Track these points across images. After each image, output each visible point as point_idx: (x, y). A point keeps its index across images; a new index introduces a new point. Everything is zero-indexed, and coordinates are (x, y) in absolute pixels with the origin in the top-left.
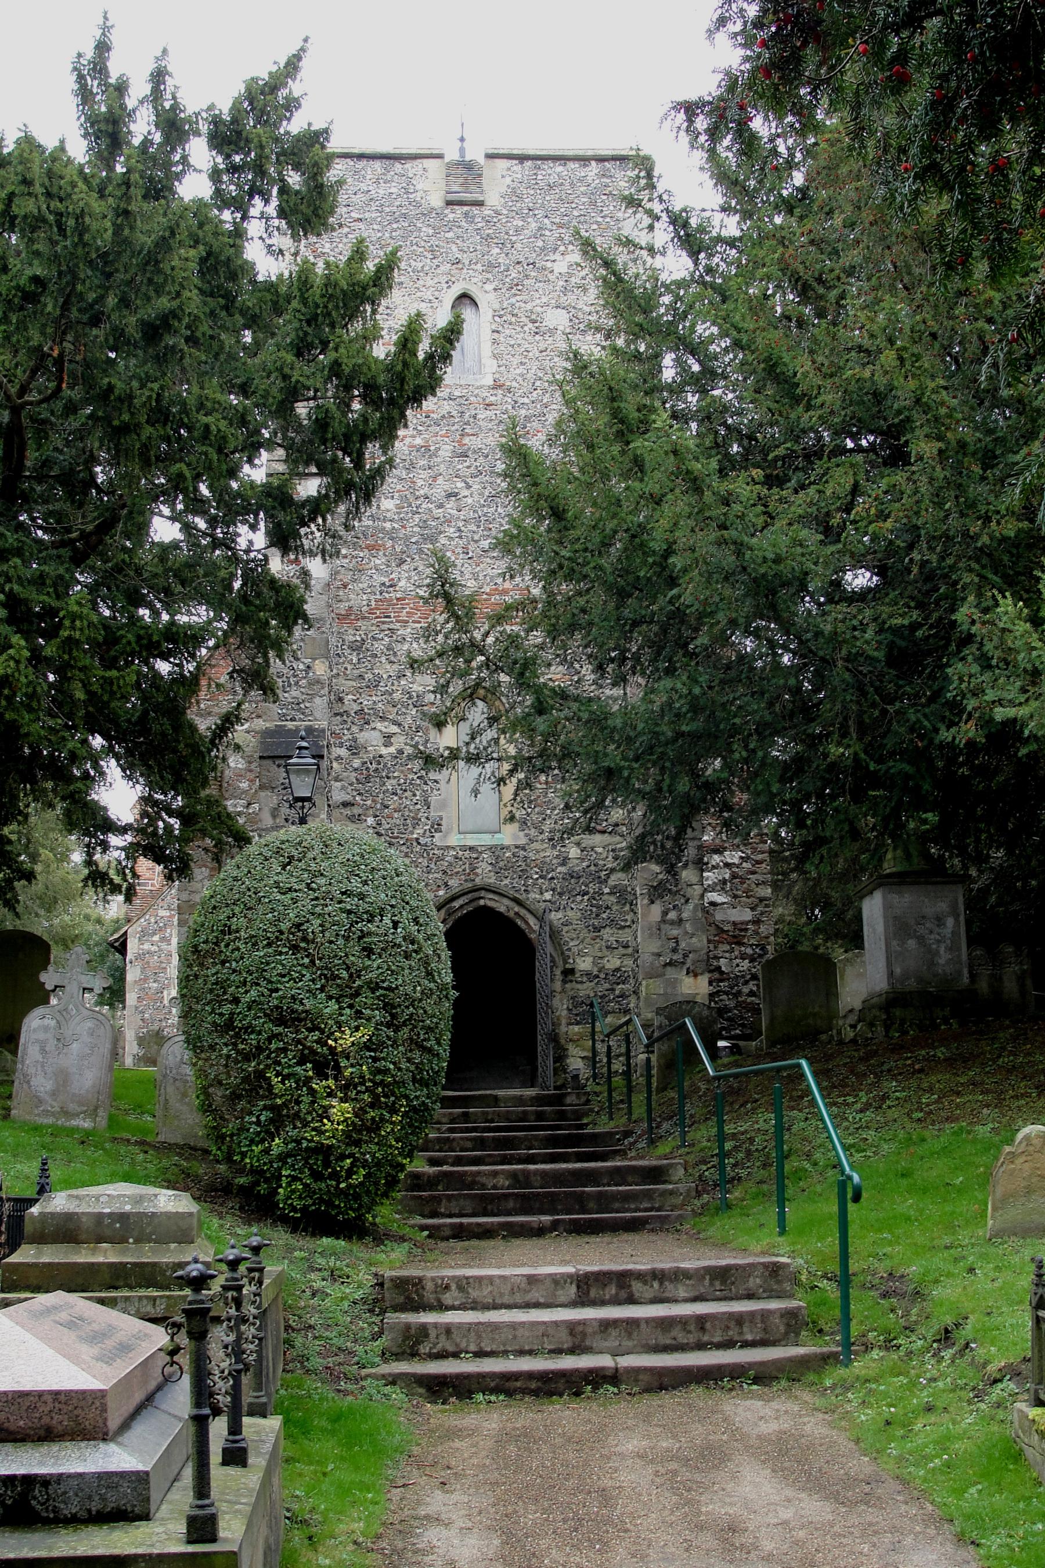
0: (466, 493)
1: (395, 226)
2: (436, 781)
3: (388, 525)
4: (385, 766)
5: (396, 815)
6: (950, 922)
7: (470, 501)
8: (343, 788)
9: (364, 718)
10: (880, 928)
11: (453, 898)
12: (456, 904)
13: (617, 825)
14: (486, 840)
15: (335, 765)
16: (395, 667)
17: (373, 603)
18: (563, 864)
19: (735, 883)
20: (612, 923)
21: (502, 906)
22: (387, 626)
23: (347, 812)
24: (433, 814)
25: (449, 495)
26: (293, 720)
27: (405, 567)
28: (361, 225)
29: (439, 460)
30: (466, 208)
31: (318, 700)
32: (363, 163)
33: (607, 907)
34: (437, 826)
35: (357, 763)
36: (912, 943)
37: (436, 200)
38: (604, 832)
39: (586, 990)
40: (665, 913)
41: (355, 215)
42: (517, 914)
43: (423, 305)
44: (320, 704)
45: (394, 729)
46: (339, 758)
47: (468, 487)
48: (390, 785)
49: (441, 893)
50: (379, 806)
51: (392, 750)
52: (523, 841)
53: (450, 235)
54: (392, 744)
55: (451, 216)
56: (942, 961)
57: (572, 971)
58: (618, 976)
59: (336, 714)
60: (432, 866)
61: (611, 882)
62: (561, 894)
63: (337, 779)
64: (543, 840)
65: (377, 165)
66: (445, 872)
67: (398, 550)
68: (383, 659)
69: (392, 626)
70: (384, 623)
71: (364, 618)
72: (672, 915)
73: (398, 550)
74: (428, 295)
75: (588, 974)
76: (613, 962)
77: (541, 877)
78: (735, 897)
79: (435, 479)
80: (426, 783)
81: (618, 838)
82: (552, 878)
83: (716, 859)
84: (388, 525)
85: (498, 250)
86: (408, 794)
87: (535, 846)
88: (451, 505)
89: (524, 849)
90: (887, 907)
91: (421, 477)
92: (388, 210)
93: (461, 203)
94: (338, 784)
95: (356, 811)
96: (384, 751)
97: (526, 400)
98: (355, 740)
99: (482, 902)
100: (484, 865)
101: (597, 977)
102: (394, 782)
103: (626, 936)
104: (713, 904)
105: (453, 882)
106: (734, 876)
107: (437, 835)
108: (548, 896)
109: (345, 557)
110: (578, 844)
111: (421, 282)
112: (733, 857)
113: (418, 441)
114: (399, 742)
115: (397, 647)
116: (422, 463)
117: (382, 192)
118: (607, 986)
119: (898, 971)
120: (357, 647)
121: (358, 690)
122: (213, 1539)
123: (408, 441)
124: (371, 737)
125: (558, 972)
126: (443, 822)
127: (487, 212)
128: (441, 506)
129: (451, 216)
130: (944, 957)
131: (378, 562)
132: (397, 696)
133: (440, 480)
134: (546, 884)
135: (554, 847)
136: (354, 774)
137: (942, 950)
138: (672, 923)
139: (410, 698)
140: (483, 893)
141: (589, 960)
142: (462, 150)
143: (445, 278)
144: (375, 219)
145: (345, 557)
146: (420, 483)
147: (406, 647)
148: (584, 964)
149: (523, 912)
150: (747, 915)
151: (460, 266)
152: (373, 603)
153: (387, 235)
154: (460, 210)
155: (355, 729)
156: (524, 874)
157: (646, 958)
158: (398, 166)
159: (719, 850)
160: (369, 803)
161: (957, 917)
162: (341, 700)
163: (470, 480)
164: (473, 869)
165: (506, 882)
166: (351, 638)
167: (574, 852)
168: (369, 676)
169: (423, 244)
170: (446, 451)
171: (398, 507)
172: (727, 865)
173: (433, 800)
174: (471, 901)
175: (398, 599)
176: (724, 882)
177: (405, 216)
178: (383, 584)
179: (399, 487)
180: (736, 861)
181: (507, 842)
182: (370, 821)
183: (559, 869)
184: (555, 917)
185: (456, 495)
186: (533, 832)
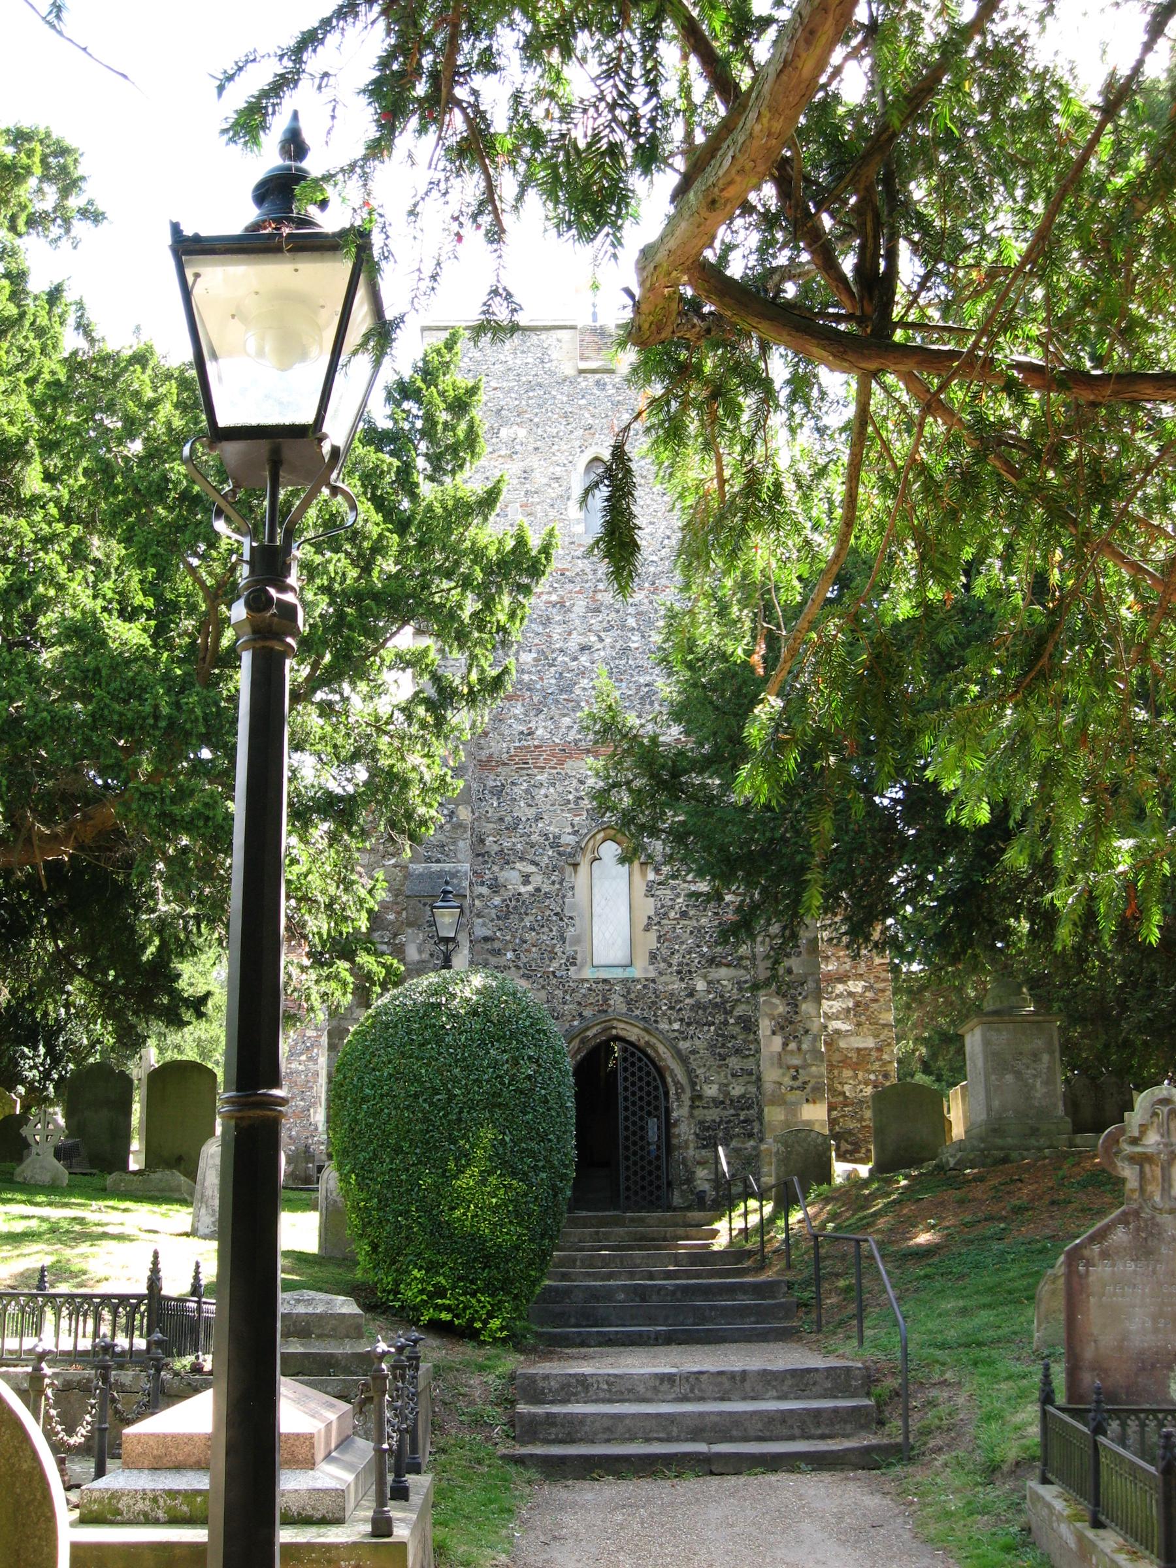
0: (600, 646)
6: (1046, 1058)
7: (602, 653)
8: (484, 925)
9: (505, 858)
10: (980, 1063)
11: (588, 1029)
12: (590, 1033)
13: (741, 958)
14: (619, 974)
15: (477, 902)
18: (691, 995)
19: (859, 1009)
20: (738, 1051)
21: (633, 1033)
25: (584, 648)
26: (438, 861)
27: (542, 716)
28: (499, 394)
29: (573, 616)
30: (598, 376)
31: (461, 844)
33: (733, 1037)
34: (572, 961)
35: (497, 901)
36: (1009, 1078)
38: (728, 965)
39: (713, 1114)
40: (785, 1044)
41: (494, 384)
42: (647, 1043)
43: (558, 469)
44: (464, 846)
45: (533, 869)
46: (481, 896)
47: (601, 640)
48: (527, 921)
49: (576, 1023)
51: (530, 888)
52: (652, 974)
53: (583, 402)
55: (584, 384)
56: (1038, 1095)
57: (700, 1097)
58: (744, 1103)
61: (736, 1013)
62: (689, 1024)
63: (479, 916)
66: (579, 1004)
67: (536, 700)
73: (536, 700)
74: (562, 459)
75: (714, 1100)
76: (737, 1090)
77: (671, 1008)
78: (859, 1024)
79: (570, 634)
81: (742, 972)
83: (840, 988)
86: (545, 929)
87: (664, 979)
88: (584, 659)
89: (654, 981)
90: (986, 1043)
91: (557, 632)
95: (497, 945)
96: (523, 889)
97: (655, 558)
98: (496, 879)
99: (614, 1032)
100: (616, 997)
101: (722, 1102)
102: (532, 918)
103: (750, 1064)
104: (837, 1032)
105: (587, 1013)
106: (857, 1004)
107: (572, 968)
108: (676, 1026)
110: (705, 977)
112: (857, 986)
113: (554, 598)
114: (537, 880)
115: (535, 792)
116: (558, 618)
117: (518, 362)
118: (732, 1112)
119: (996, 1103)
120: (498, 792)
121: (499, 833)
122: (390, 1535)
123: (544, 597)
124: (511, 877)
126: (579, 956)
128: (575, 659)
129: (584, 384)
130: (1040, 1090)
132: (535, 838)
133: (574, 634)
134: (673, 1014)
135: (682, 980)
137: (1038, 1084)
138: (792, 1052)
140: (615, 1023)
141: (715, 1087)
142: (594, 314)
143: (577, 443)
146: (556, 637)
147: (543, 791)
148: (711, 1091)
150: (870, 1043)
154: (592, 378)
155: (495, 868)
157: (768, 1087)
159: (842, 978)
161: (1051, 1053)
162: (482, 841)
163: (602, 634)
164: (606, 1000)
166: (492, 784)
167: (701, 985)
168: (508, 819)
170: (580, 606)
171: (535, 660)
172: (851, 994)
173: (568, 935)
174: (605, 1030)
176: (848, 1010)
179: (536, 641)
180: (859, 990)
182: (510, 955)
183: (688, 1001)
184: (684, 1045)
185: (590, 648)
186: (663, 965)
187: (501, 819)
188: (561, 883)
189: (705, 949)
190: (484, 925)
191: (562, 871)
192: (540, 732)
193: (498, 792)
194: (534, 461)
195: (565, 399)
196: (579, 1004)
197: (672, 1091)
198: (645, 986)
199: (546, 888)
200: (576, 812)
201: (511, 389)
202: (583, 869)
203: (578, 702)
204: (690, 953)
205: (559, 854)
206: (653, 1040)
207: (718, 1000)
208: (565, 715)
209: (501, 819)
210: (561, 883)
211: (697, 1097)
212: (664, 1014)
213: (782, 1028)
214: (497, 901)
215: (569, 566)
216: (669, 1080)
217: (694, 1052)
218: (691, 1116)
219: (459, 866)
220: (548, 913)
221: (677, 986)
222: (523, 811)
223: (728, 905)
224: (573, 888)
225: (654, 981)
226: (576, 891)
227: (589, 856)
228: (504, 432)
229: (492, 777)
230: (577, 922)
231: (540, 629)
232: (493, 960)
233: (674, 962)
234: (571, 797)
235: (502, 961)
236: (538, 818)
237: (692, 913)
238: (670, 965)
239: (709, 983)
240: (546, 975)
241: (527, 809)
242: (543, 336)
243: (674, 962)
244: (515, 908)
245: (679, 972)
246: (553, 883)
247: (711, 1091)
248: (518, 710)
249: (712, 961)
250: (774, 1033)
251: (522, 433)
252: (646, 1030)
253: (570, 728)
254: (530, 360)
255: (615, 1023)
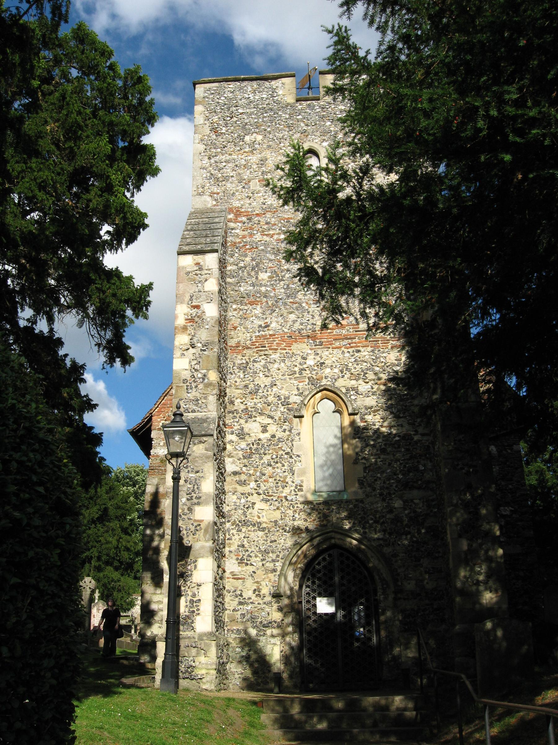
1: (265, 115)
2: (299, 456)
3: (263, 289)
4: (263, 445)
5: (270, 480)
15: (228, 447)
16: (270, 379)
17: (254, 339)
18: (391, 511)
22: (263, 353)
23: (237, 478)
24: (297, 481)
26: (193, 411)
27: (274, 314)
30: (309, 102)
32: (245, 83)
35: (243, 445)
37: (290, 99)
38: (419, 488)
41: (240, 111)
45: (270, 421)
46: (231, 442)
48: (266, 459)
50: (258, 474)
51: (267, 435)
52: (361, 496)
53: (300, 117)
54: (267, 431)
55: (300, 107)
59: (229, 412)
60: (297, 515)
63: (230, 456)
64: (375, 495)
65: (255, 84)
67: (270, 303)
68: (261, 375)
69: (266, 353)
70: (261, 351)
71: (249, 348)
73: (270, 303)
80: (291, 457)
82: (383, 523)
84: (263, 289)
85: (330, 123)
86: (279, 465)
92: (260, 106)
93: (306, 100)
94: (231, 460)
95: (243, 477)
96: (262, 436)
99: (333, 541)
109: (235, 310)
110: (401, 497)
111: (282, 145)
114: (272, 429)
115: (270, 366)
117: (257, 97)
120: (244, 368)
121: (244, 396)
123: (276, 237)
124: (253, 428)
127: (322, 103)
129: (300, 107)
131: (257, 312)
132: (270, 399)
136: (241, 453)
139: (280, 400)
140: (333, 534)
141: (413, 582)
144: (253, 113)
145: (235, 310)
147: (276, 366)
151: (306, 134)
152: (254, 339)
153: (260, 120)
154: (304, 103)
155: (242, 421)
158: (267, 84)
160: (251, 472)
162: (232, 403)
167: (398, 504)
168: (251, 386)
169: (283, 123)
171: (270, 277)
175: (270, 335)
177: (271, 109)
178: (260, 326)
179: (270, 265)
180: (508, 513)
182: (253, 485)
183: (388, 516)
184: (387, 550)
187: (246, 386)
188: (290, 431)
189: (400, 476)
190: (234, 462)
191: (291, 422)
192: (273, 325)
193: (244, 368)
194: (267, 154)
195: (287, 116)
197: (379, 587)
198: (355, 506)
199: (279, 434)
200: (300, 379)
201: (252, 113)
202: (307, 419)
203: (300, 304)
204: (389, 479)
205: (288, 410)
207: (412, 515)
208: (291, 313)
209: (246, 386)
210: (290, 431)
214: (243, 445)
215: (293, 216)
216: (377, 577)
219: (209, 414)
220: (281, 452)
221: (379, 506)
222: (262, 380)
223: (416, 442)
224: (299, 434)
225: (362, 501)
226: (301, 436)
227: (311, 411)
228: (247, 138)
229: (239, 357)
230: (303, 458)
231: (273, 257)
232: (240, 489)
233: (378, 487)
234: (296, 369)
235: (247, 489)
236: (273, 385)
237: (389, 449)
238: (374, 489)
239: (405, 502)
240: (279, 500)
241: (264, 379)
242: (273, 82)
243: (378, 487)
244: (256, 449)
246: (284, 431)
247: (410, 586)
248: (258, 310)
249: (406, 485)
250: (460, 536)
251: (259, 138)
253: (294, 322)
254: (265, 96)
255: (333, 534)
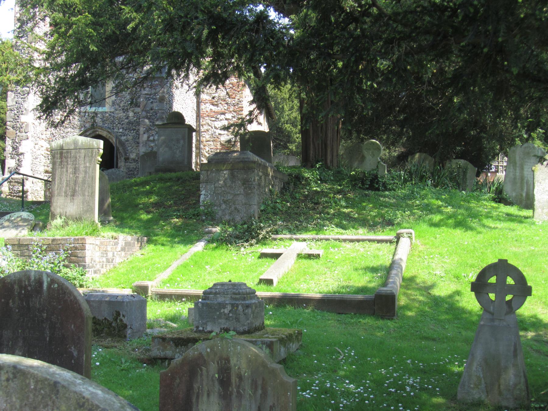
39: (133, 165)
40: (149, 137)
52: (113, 110)
56: (177, 156)
62: (126, 130)
66: (84, 121)
72: (151, 138)
75: (134, 160)
77: (119, 123)
82: (123, 124)
83: (223, 117)
87: (117, 112)
89: (113, 113)
99: (97, 133)
101: (137, 161)
108: (121, 130)
110: (133, 111)
112: (229, 116)
125: (123, 159)
135: (124, 112)
137: (178, 152)
138: (151, 141)
141: (135, 154)
149: (111, 136)
156: (113, 122)
159: (224, 114)
165: (106, 125)
167: (131, 114)
172: (226, 119)
174: (93, 132)
180: (231, 118)
181: (106, 111)
184: (123, 138)
186: (117, 107)
196: (84, 121)
198: (110, 115)
206: (111, 136)
211: (127, 159)
212: (116, 126)
213: (148, 131)
217: (127, 141)
218: (125, 166)
225: (113, 113)
233: (121, 105)
239: (135, 113)
243: (121, 105)
245: (123, 109)
247: (133, 156)
250: (144, 133)
252: (108, 132)
255: (97, 129)
